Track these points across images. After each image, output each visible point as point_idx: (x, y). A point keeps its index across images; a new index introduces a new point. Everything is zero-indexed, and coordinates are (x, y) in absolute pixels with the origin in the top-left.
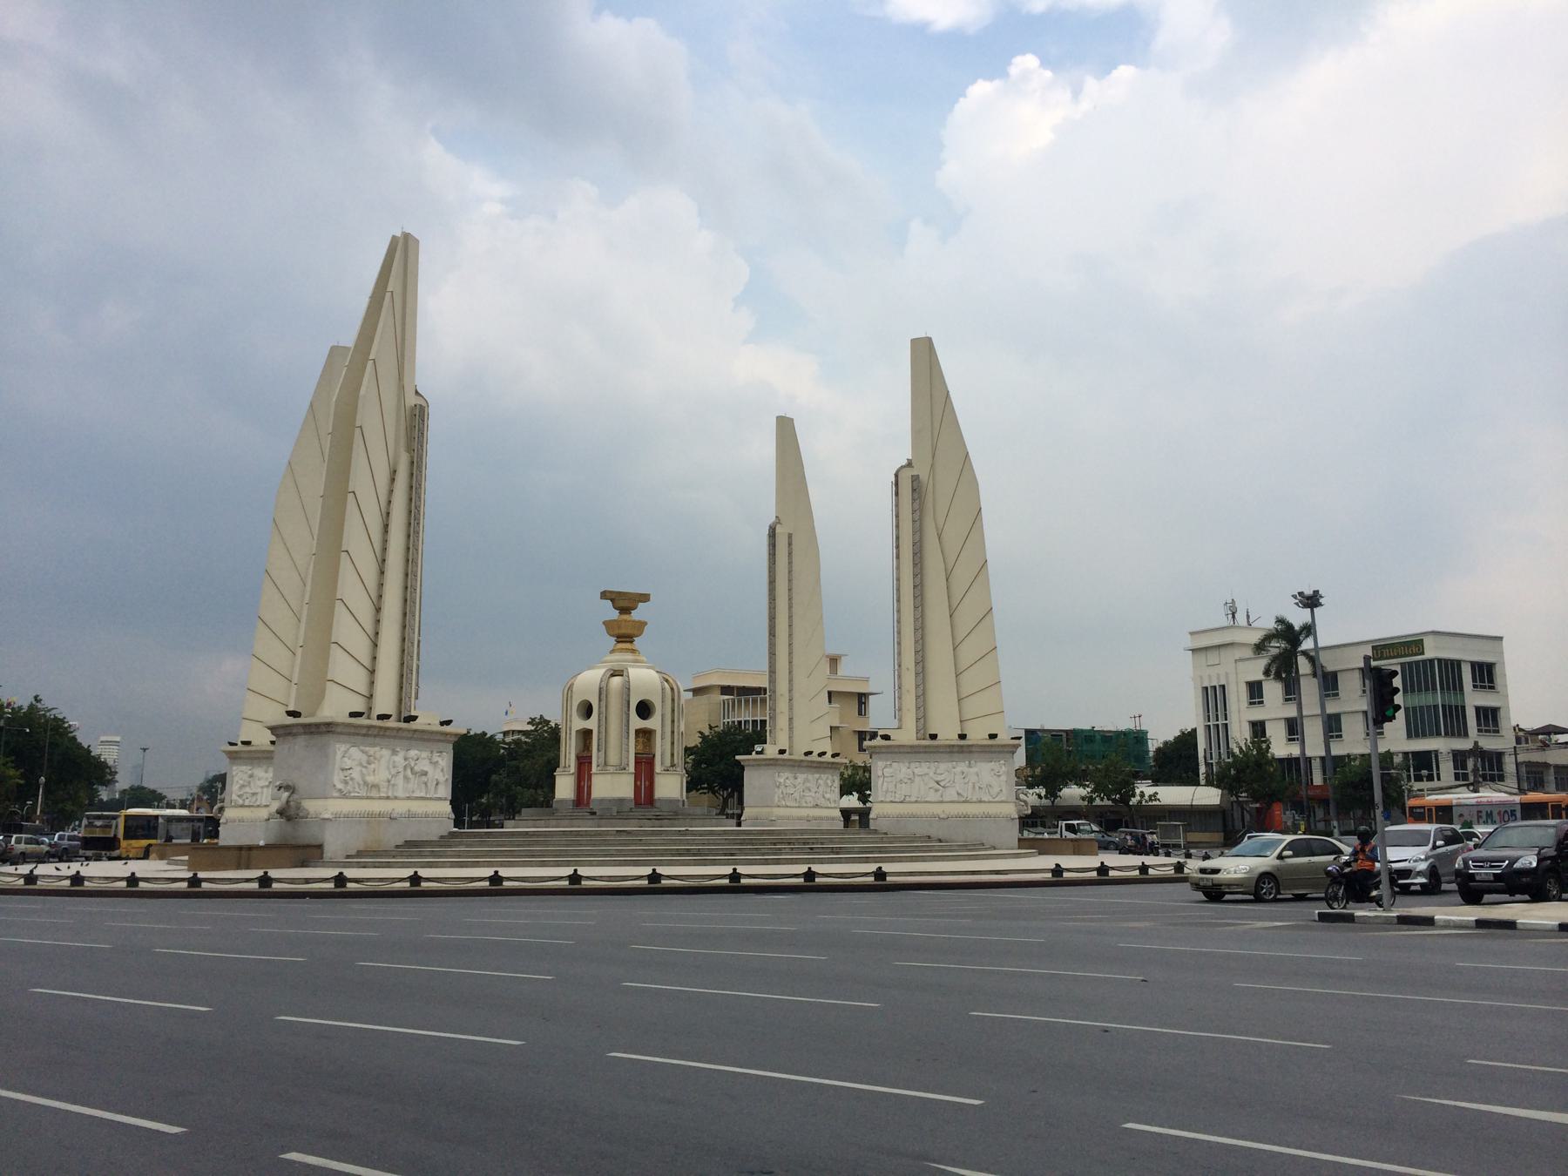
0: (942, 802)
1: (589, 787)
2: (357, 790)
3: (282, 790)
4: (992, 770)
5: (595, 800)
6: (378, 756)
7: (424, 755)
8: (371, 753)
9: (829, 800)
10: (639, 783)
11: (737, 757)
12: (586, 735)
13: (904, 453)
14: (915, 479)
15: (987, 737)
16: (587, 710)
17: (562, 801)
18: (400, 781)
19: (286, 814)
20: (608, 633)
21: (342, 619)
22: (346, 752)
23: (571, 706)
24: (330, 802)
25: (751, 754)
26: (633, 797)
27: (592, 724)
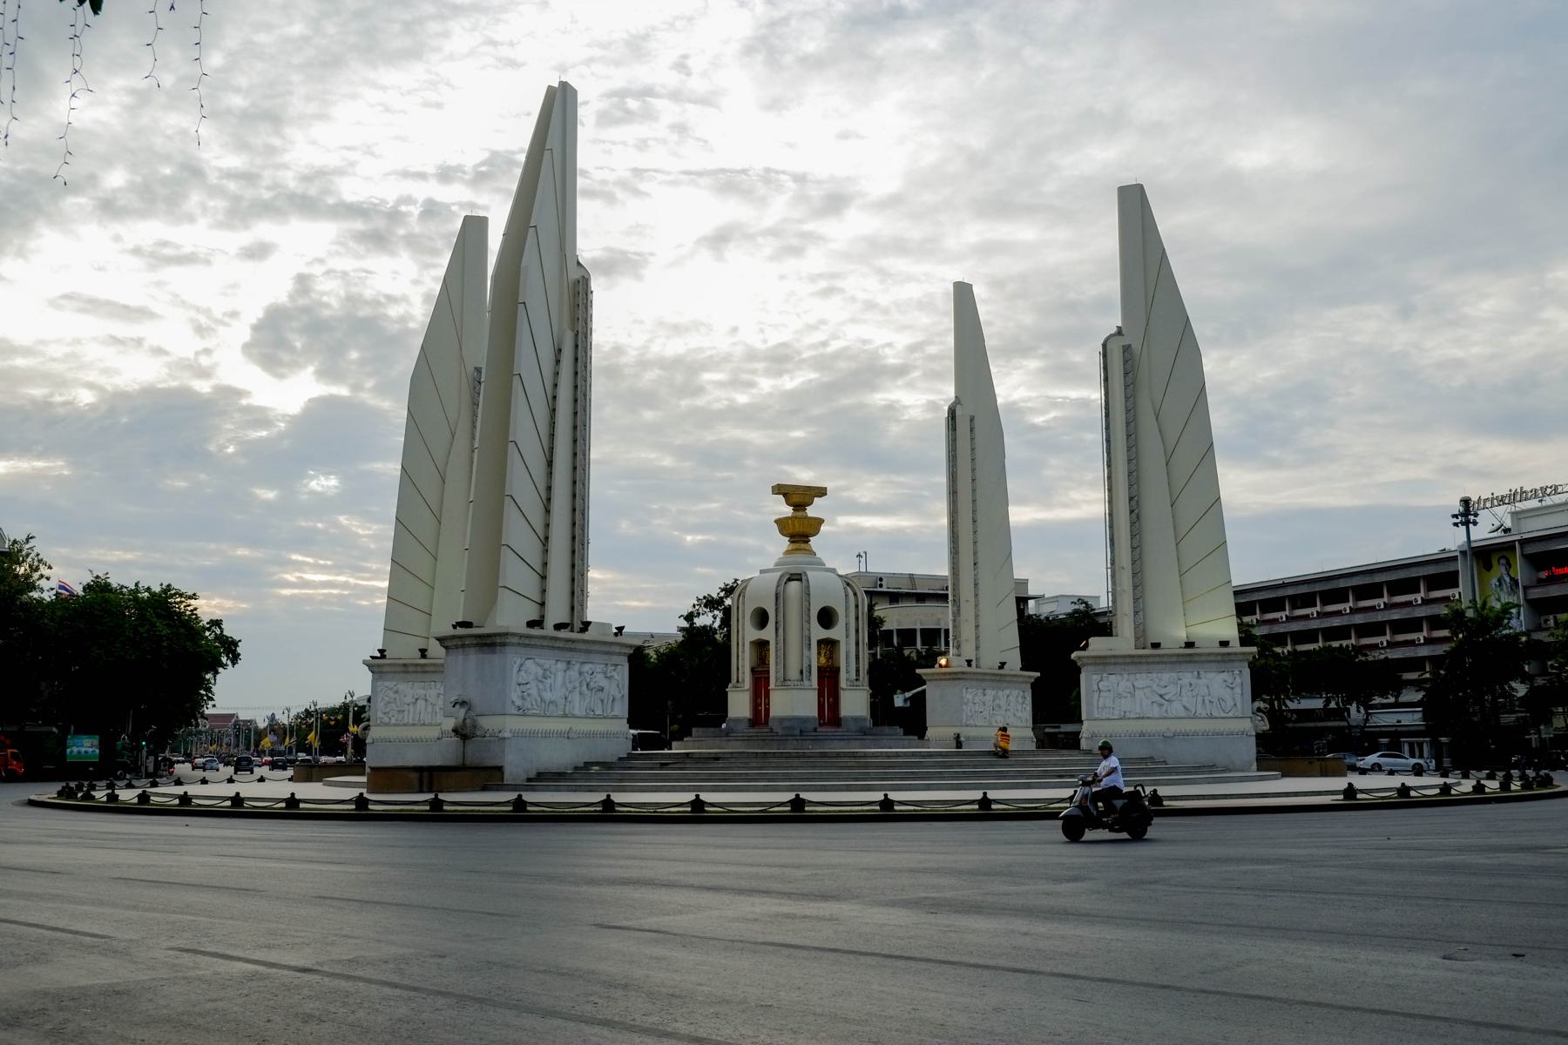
0: (1165, 718)
1: (767, 704)
2: (535, 707)
3: (458, 706)
4: (1225, 681)
5: (774, 718)
6: (553, 670)
7: (599, 668)
8: (547, 666)
9: (1020, 718)
11: (918, 671)
12: (761, 646)
13: (1114, 321)
14: (1127, 349)
15: (1218, 645)
16: (761, 618)
17: (738, 720)
18: (576, 696)
19: (463, 733)
21: (512, 517)
22: (521, 665)
24: (508, 718)
25: (934, 667)
26: (817, 715)
27: (768, 633)
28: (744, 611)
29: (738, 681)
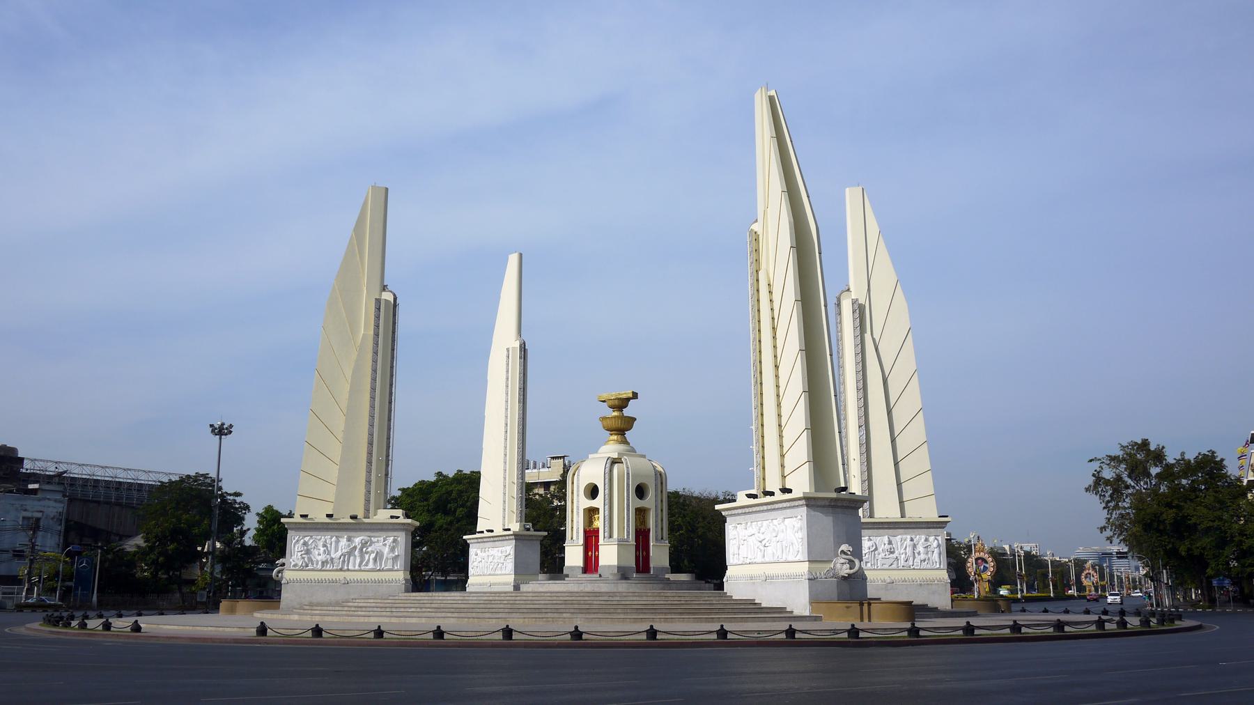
12: (591, 513)
17: (572, 568)
20: (604, 428)
27: (598, 503)
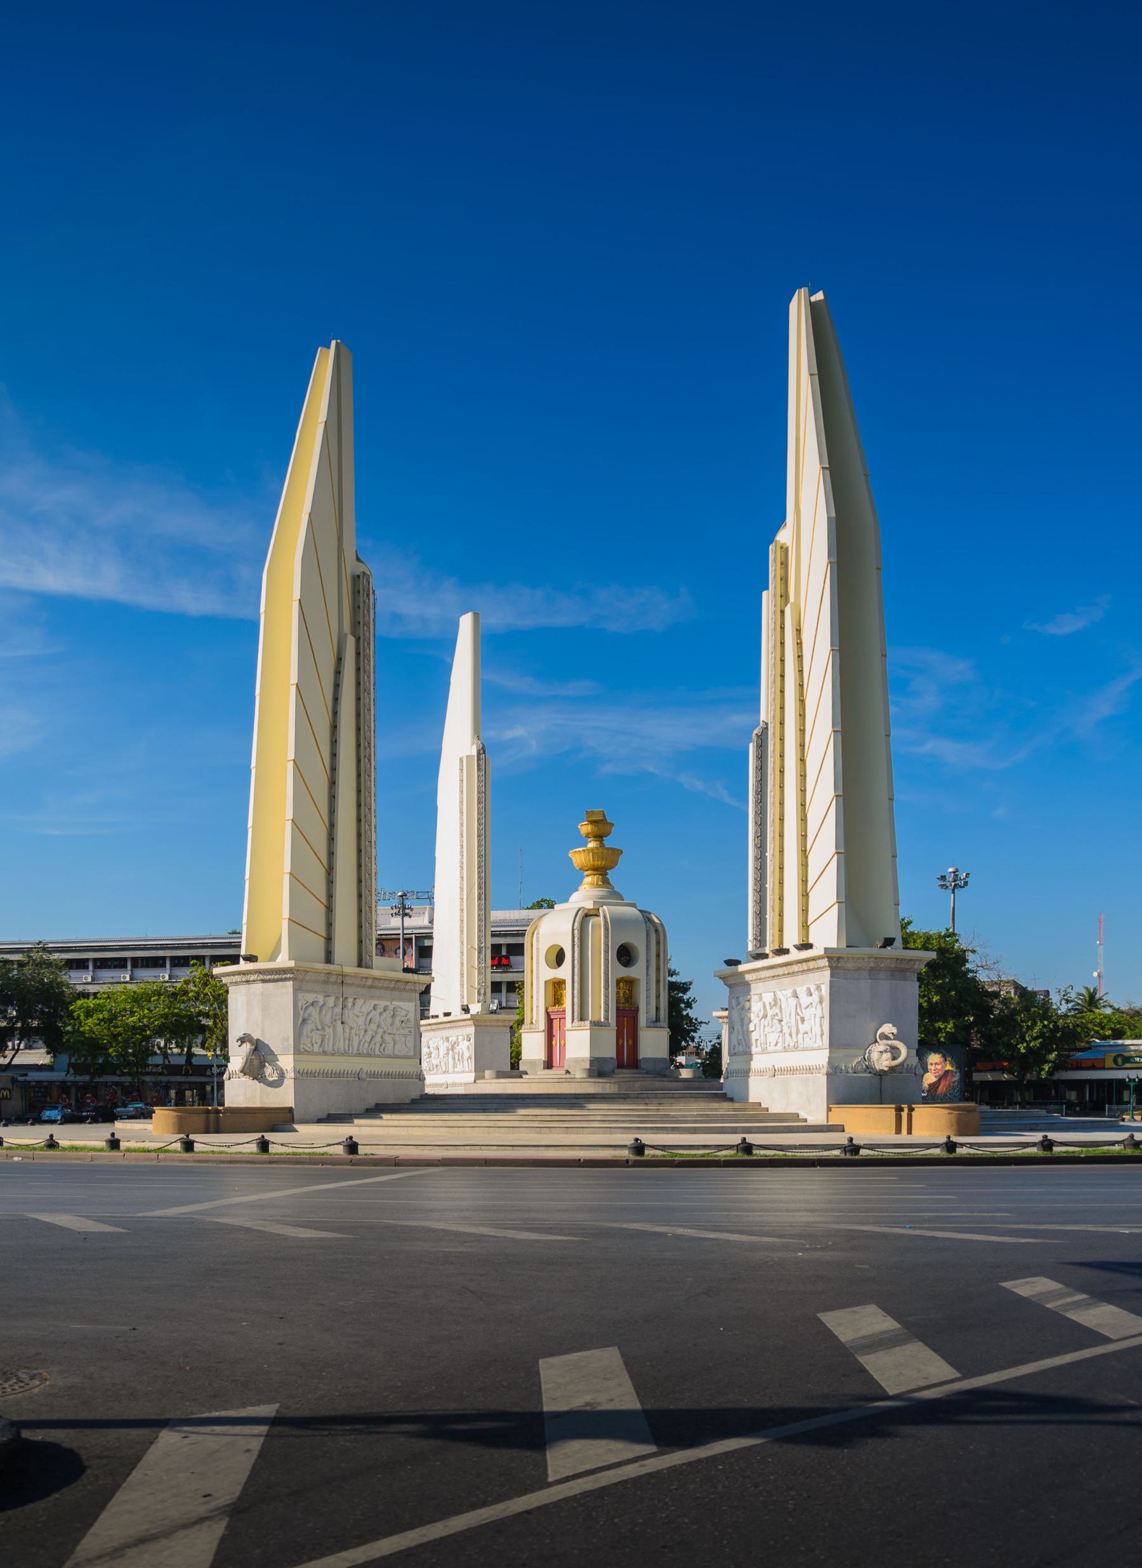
10: (621, 1041)
17: (532, 1063)
23: (538, 952)
26: (615, 1057)
27: (564, 972)
28: (538, 949)
29: (532, 1023)
